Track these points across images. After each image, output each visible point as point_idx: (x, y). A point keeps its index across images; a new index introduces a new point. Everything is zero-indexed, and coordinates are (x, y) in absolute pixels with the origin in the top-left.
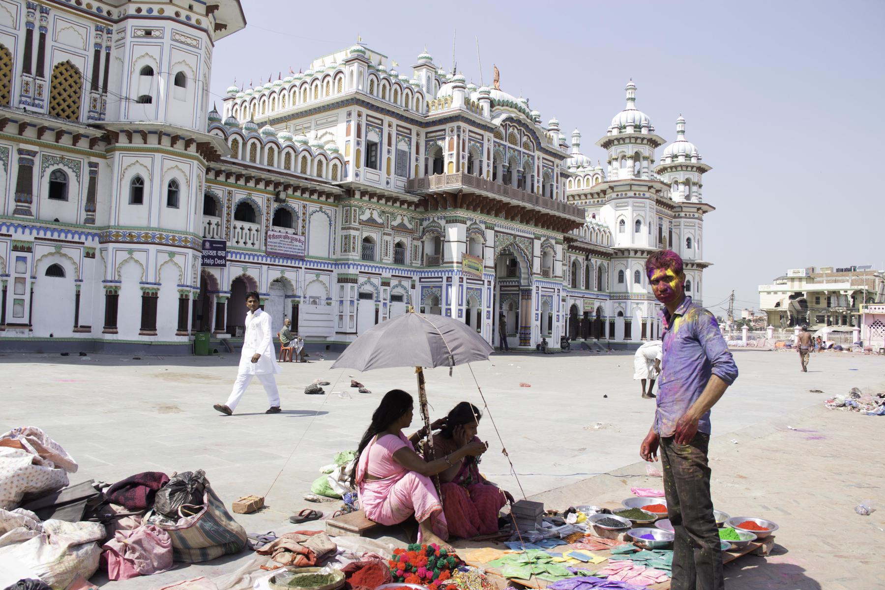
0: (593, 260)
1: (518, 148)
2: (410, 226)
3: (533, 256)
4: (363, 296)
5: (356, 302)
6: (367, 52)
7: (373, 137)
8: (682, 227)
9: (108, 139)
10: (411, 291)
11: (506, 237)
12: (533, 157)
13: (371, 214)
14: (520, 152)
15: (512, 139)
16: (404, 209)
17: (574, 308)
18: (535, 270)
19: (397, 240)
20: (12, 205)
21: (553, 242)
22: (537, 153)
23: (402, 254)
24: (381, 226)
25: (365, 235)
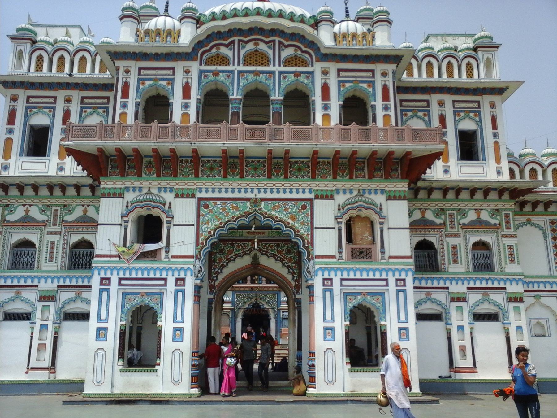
1: (270, 68)
3: (312, 228)
7: (40, 120)
11: (229, 204)
12: (312, 73)
13: (27, 211)
14: (273, 73)
15: (256, 58)
16: (86, 197)
18: (318, 250)
19: (75, 238)
21: (379, 199)
22: (318, 67)
24: (44, 224)
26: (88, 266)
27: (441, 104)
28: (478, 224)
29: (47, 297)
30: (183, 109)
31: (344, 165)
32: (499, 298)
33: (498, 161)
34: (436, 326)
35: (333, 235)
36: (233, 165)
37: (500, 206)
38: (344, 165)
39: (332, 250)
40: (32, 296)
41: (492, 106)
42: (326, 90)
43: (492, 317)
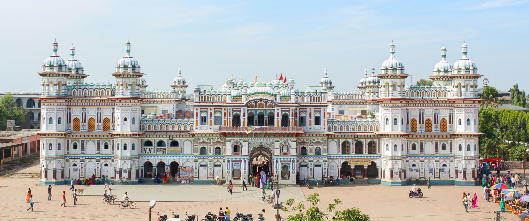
0: (363, 140)
2: (222, 142)
4: (201, 166)
5: (198, 169)
6: (201, 87)
7: (204, 114)
8: (455, 112)
9: (112, 135)
10: (223, 163)
15: (261, 105)
17: (345, 164)
19: (216, 146)
20: (96, 152)
21: (290, 142)
22: (276, 108)
23: (220, 151)
24: (208, 143)
25: (201, 147)
26: (219, 153)
27: (310, 109)
28: (318, 142)
29: (210, 161)
30: (244, 120)
31: (281, 135)
32: (321, 161)
33: (324, 125)
34: (305, 168)
35: (279, 150)
36: (256, 135)
37: (324, 138)
38: (281, 135)
39: (278, 154)
40: (207, 161)
41: (324, 110)
42: (278, 114)
43: (319, 166)
